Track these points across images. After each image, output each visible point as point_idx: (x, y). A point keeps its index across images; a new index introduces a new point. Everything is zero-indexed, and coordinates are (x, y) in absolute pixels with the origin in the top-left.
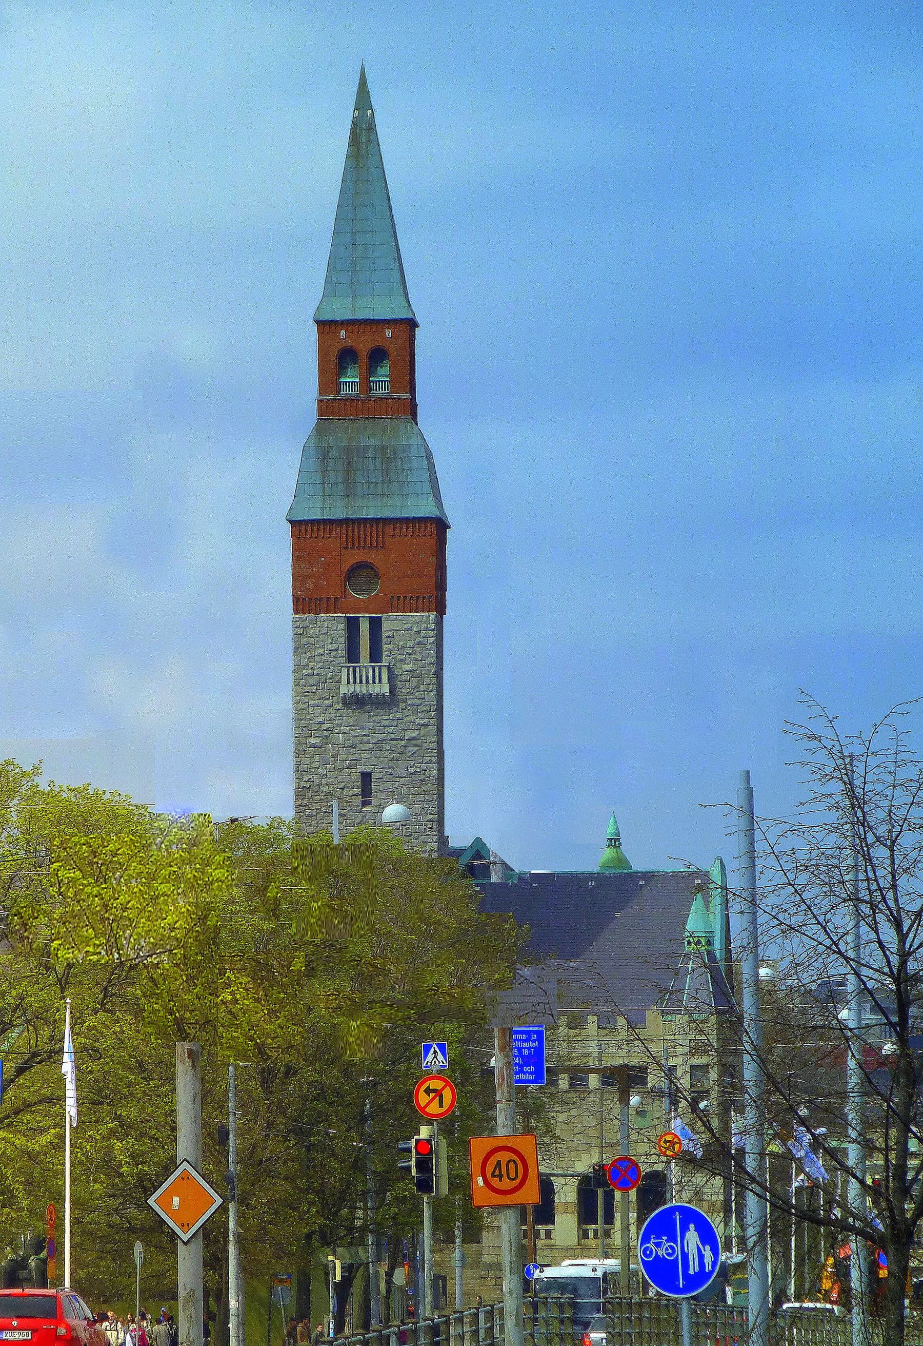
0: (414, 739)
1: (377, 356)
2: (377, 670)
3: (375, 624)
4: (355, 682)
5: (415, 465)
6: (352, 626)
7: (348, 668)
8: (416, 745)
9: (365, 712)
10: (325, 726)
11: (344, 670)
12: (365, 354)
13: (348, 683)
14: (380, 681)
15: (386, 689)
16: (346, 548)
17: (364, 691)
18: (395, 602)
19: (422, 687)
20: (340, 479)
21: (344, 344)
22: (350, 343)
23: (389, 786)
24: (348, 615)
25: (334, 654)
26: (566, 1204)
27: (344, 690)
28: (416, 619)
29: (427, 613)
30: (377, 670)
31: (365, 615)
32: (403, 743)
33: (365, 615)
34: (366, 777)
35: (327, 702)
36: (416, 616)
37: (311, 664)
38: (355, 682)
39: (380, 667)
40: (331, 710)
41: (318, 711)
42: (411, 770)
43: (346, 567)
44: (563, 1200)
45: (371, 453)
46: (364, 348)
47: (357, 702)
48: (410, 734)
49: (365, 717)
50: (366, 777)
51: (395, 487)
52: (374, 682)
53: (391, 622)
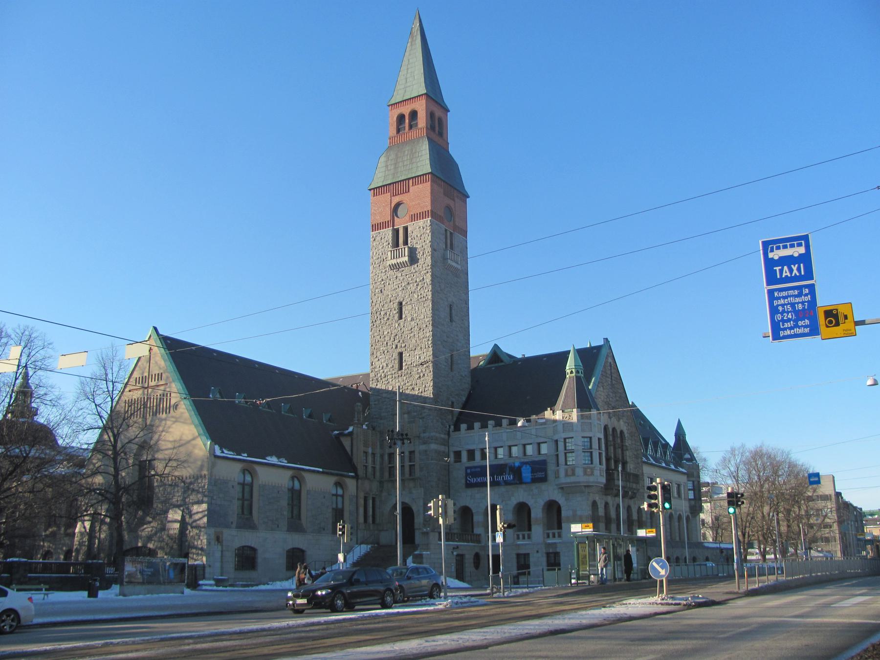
3: (406, 229)
6: (396, 232)
7: (391, 251)
9: (400, 272)
10: (382, 283)
11: (389, 253)
12: (408, 114)
16: (393, 196)
19: (425, 256)
20: (392, 167)
23: (410, 307)
24: (395, 228)
47: (395, 267)
50: (400, 304)
51: (414, 165)
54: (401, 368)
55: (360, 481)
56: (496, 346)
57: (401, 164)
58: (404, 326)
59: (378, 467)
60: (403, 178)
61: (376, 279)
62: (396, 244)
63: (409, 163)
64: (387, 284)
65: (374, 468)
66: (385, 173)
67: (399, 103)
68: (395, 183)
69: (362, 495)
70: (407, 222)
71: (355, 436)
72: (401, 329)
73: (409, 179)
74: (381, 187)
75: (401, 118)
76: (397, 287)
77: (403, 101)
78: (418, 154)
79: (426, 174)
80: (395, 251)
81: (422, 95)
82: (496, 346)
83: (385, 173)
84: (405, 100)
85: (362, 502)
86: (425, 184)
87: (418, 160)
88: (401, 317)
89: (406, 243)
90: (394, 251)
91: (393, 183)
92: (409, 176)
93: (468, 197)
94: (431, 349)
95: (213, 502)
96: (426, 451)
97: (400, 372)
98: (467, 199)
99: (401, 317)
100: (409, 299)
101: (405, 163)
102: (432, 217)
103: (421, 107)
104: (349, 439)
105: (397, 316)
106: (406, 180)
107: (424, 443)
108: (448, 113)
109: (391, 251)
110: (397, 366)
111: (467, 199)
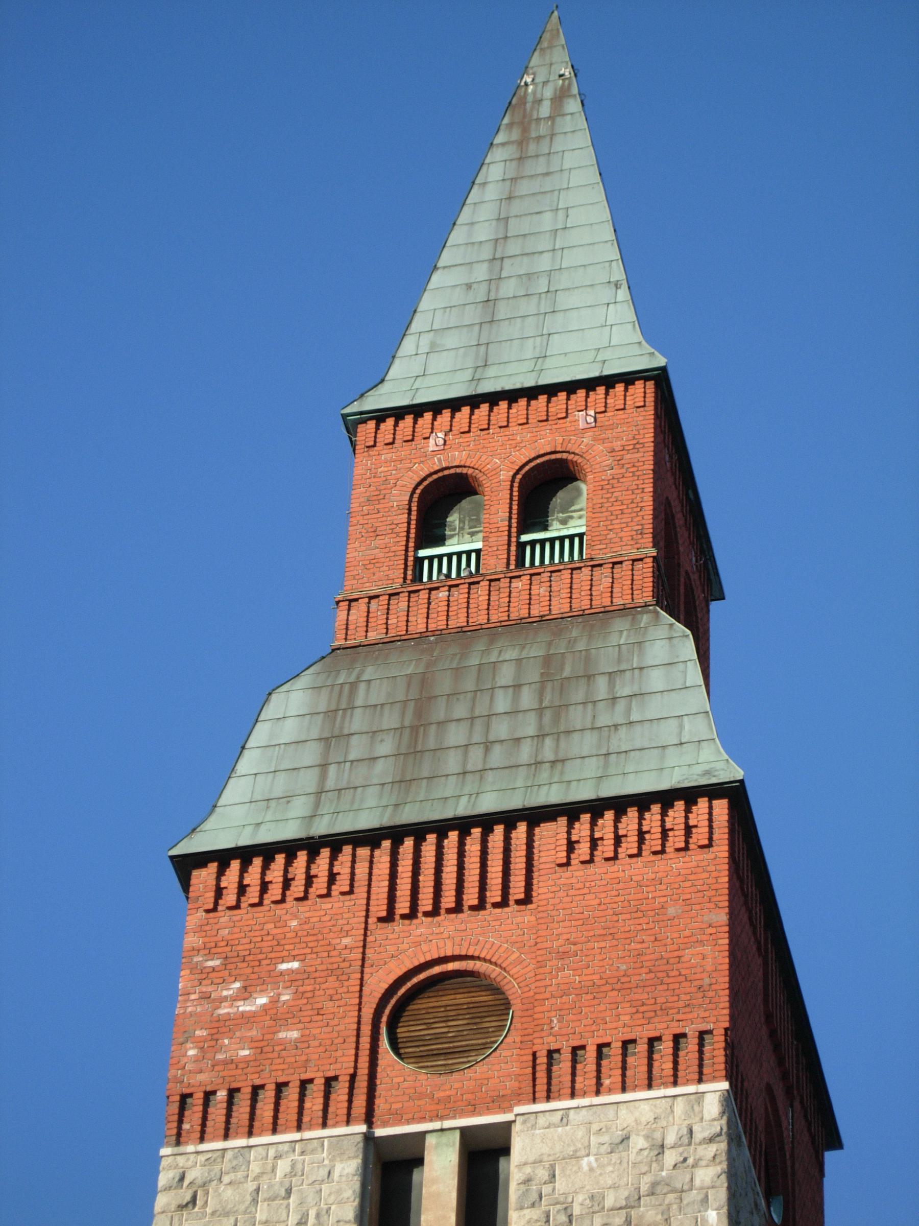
5: (656, 680)
12: (505, 475)
18: (563, 1067)
20: (386, 747)
21: (436, 464)
24: (380, 1132)
28: (646, 1112)
29: (691, 1089)
31: (447, 1124)
33: (447, 1124)
43: (377, 983)
45: (506, 675)
51: (586, 743)
57: (456, 735)
60: (488, 803)
63: (531, 730)
66: (323, 777)
67: (436, 407)
68: (419, 831)
70: (501, 1102)
74: (290, 848)
77: (473, 401)
81: (628, 379)
83: (323, 777)
84: (493, 399)
86: (675, 864)
87: (604, 719)
91: (396, 834)
92: (552, 795)
93: (835, 1142)
98: (830, 1157)
101: (501, 729)
106: (509, 819)
108: (715, 607)
111: (830, 1157)
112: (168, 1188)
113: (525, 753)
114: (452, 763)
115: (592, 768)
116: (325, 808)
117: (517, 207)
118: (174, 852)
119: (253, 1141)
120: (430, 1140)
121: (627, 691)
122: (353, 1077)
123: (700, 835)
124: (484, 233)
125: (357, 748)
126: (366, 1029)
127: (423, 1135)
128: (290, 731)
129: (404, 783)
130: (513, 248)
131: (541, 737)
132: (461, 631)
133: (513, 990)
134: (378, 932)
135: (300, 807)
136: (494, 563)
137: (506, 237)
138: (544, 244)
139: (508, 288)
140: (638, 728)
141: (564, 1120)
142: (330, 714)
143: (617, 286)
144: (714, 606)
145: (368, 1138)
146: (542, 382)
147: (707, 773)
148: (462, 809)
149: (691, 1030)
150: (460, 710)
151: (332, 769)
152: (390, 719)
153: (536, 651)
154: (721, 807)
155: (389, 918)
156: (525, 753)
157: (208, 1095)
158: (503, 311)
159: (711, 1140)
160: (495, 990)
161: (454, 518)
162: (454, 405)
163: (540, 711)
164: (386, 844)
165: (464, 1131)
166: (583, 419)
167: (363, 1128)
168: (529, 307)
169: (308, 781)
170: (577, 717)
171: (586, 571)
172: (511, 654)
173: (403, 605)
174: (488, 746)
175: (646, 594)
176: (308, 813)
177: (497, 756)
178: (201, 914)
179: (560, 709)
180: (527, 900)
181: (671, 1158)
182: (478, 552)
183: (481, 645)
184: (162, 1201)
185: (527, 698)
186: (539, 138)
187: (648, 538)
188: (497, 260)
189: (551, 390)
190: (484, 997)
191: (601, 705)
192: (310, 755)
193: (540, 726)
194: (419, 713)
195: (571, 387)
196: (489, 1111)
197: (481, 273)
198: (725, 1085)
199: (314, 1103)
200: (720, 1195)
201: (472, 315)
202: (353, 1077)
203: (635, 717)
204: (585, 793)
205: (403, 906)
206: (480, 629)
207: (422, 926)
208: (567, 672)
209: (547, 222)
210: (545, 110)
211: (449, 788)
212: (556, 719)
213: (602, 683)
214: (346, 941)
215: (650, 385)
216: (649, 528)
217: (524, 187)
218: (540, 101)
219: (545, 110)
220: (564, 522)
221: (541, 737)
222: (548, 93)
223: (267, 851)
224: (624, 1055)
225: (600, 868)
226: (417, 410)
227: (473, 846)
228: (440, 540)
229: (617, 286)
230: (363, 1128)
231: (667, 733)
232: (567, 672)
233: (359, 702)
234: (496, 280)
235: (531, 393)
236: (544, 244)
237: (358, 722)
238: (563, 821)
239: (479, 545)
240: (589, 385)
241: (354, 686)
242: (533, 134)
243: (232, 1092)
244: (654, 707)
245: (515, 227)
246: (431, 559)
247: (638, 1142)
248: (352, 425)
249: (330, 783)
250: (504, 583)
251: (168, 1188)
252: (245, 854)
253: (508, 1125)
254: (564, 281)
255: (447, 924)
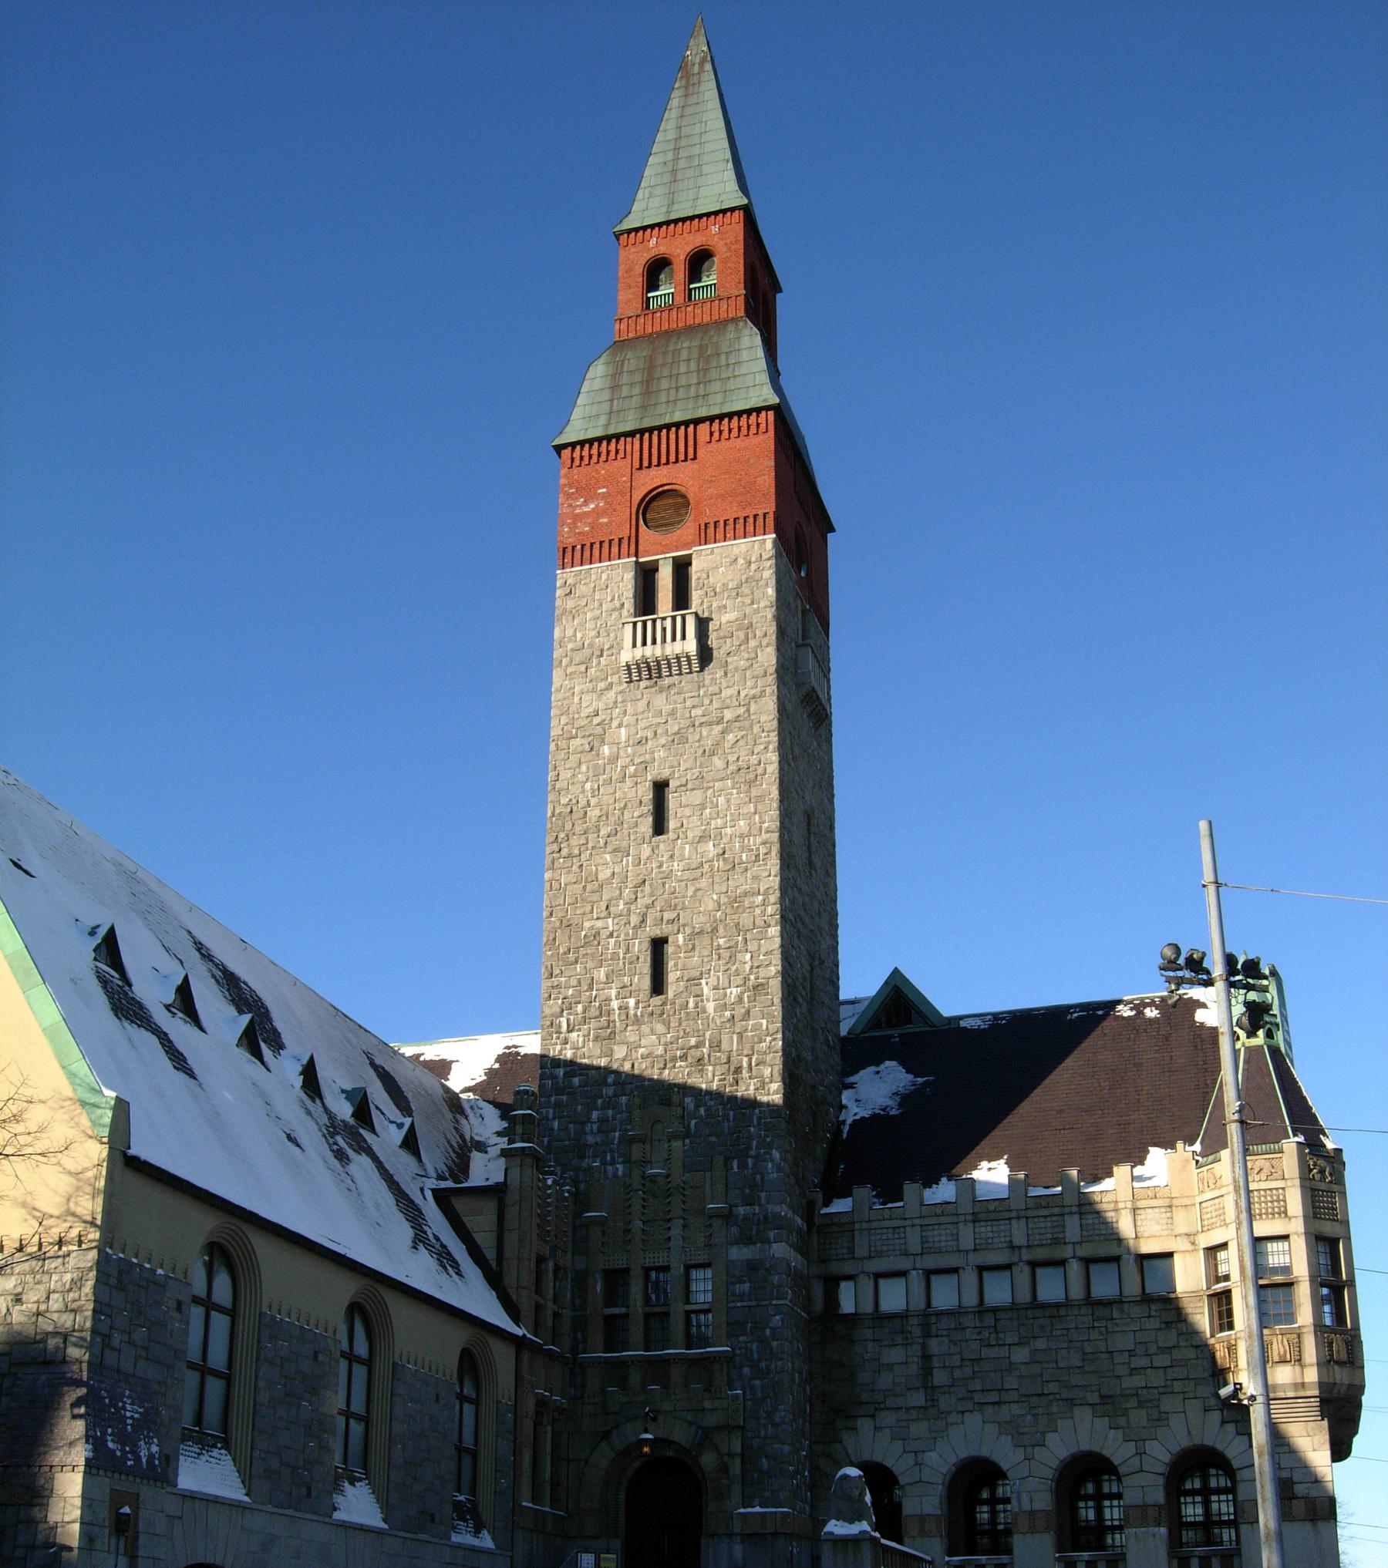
0: (737, 719)
1: (699, 261)
2: (679, 620)
3: (682, 568)
4: (644, 643)
5: (745, 356)
8: (740, 729)
10: (596, 720)
11: (629, 628)
12: (682, 257)
13: (634, 645)
14: (684, 637)
15: (691, 646)
17: (658, 652)
18: (711, 530)
19: (752, 643)
20: (636, 391)
22: (662, 250)
23: (696, 797)
24: (641, 560)
25: (616, 614)
26: (1032, 1513)
27: (627, 655)
28: (744, 548)
29: (761, 538)
30: (679, 620)
31: (667, 555)
32: (719, 728)
33: (667, 555)
34: (660, 788)
35: (602, 685)
36: (741, 546)
37: (579, 635)
38: (644, 643)
39: (683, 617)
40: (611, 694)
41: (586, 698)
42: (732, 768)
43: (637, 496)
44: (1026, 1507)
45: (684, 355)
46: (679, 248)
47: (651, 671)
48: (728, 715)
49: (660, 701)
50: (660, 788)
51: (716, 386)
52: (674, 639)
53: (705, 560)
54: (658, 986)
55: (525, 1357)
56: (896, 972)
57: (664, 384)
58: (672, 856)
59: (567, 1313)
60: (678, 417)
61: (573, 708)
62: (646, 602)
63: (695, 381)
64: (615, 723)
65: (556, 1315)
66: (612, 405)
67: (652, 227)
68: (651, 430)
69: (529, 1405)
70: (687, 546)
71: (512, 1197)
72: (660, 866)
73: (697, 422)
74: (599, 440)
75: (656, 270)
76: (650, 735)
77: (668, 223)
78: (727, 358)
79: (758, 410)
80: (649, 625)
81: (732, 210)
82: (896, 972)
83: (612, 405)
84: (676, 221)
85: (528, 1425)
86: (753, 440)
88: (659, 828)
89: (681, 600)
90: (644, 623)
91: (642, 432)
92: (703, 412)
94: (774, 931)
95: (110, 1358)
96: (752, 1267)
97: (657, 1000)
98: (829, 535)
99: (659, 828)
100: (696, 771)
101: (683, 381)
102: (778, 530)
103: (727, 239)
104: (490, 1206)
105: (647, 825)
106: (686, 423)
107: (746, 1240)
109: (635, 624)
110: (646, 983)
111: (829, 535)
112: (561, 587)
113: (692, 392)
114: (663, 398)
115: (718, 398)
116: (613, 420)
117: (686, 121)
118: (554, 444)
119: (592, 566)
120: (661, 562)
121: (733, 361)
122: (629, 538)
123: (763, 427)
124: (671, 135)
125: (625, 391)
126: (634, 517)
127: (658, 560)
128: (598, 384)
129: (644, 407)
130: (683, 143)
131: (699, 383)
132: (666, 332)
133: (691, 497)
134: (637, 474)
135: (603, 420)
136: (679, 300)
137: (680, 137)
138: (696, 140)
139: (682, 163)
140: (737, 378)
141: (712, 552)
142: (614, 376)
143: (728, 161)
144: (778, 296)
145: (637, 563)
146: (696, 213)
147: (765, 400)
148: (667, 420)
149: (760, 513)
150: (666, 373)
151: (615, 401)
152: (637, 378)
153: (696, 343)
154: (771, 414)
155: (640, 468)
156: (692, 392)
157: (574, 547)
158: (679, 176)
159: (769, 559)
160: (684, 497)
161: (662, 276)
162: (660, 225)
163: (698, 371)
164: (638, 436)
165: (673, 558)
166: (715, 229)
167: (634, 559)
168: (690, 173)
169: (606, 408)
170: (713, 374)
171: (717, 302)
172: (686, 344)
173: (642, 320)
174: (677, 389)
175: (741, 313)
176: (606, 423)
177: (681, 393)
178: (566, 469)
179: (706, 371)
180: (695, 458)
181: (753, 567)
182: (673, 293)
183: (674, 340)
184: (558, 593)
185: (693, 366)
186: (694, 84)
187: (742, 286)
188: (677, 149)
189: (700, 216)
190: (680, 500)
191: (723, 368)
192: (606, 395)
193: (698, 378)
194: (649, 374)
195: (708, 215)
196: (683, 550)
197: (670, 156)
198: (774, 536)
199: (615, 549)
200: (773, 582)
201: (667, 178)
202: (629, 538)
203: (736, 374)
204: (716, 411)
205: (646, 463)
206: (674, 330)
207: (653, 471)
208: (709, 353)
209: (697, 129)
210: (696, 70)
211: (661, 409)
212: (705, 375)
213: (723, 357)
214: (624, 479)
215: (741, 211)
216: (742, 281)
217: (688, 111)
218: (694, 64)
219: (696, 70)
220: (708, 276)
221: (699, 383)
222: (698, 61)
223: (591, 442)
224: (735, 524)
225: (723, 443)
226: (644, 228)
227: (673, 436)
228: (656, 288)
229: (728, 161)
230: (634, 559)
231: (749, 381)
232: (709, 353)
233: (625, 369)
234: (676, 159)
235: (692, 218)
236: (696, 140)
237: (625, 379)
238: (708, 423)
239: (673, 290)
240: (716, 213)
241: (623, 361)
242: (691, 82)
243: (583, 546)
244: (744, 369)
245: (685, 132)
246: (653, 297)
247: (741, 561)
248: (617, 236)
249: (615, 409)
250: (683, 309)
251: (561, 587)
252: (582, 443)
253: (691, 555)
254: (705, 159)
255: (664, 470)
